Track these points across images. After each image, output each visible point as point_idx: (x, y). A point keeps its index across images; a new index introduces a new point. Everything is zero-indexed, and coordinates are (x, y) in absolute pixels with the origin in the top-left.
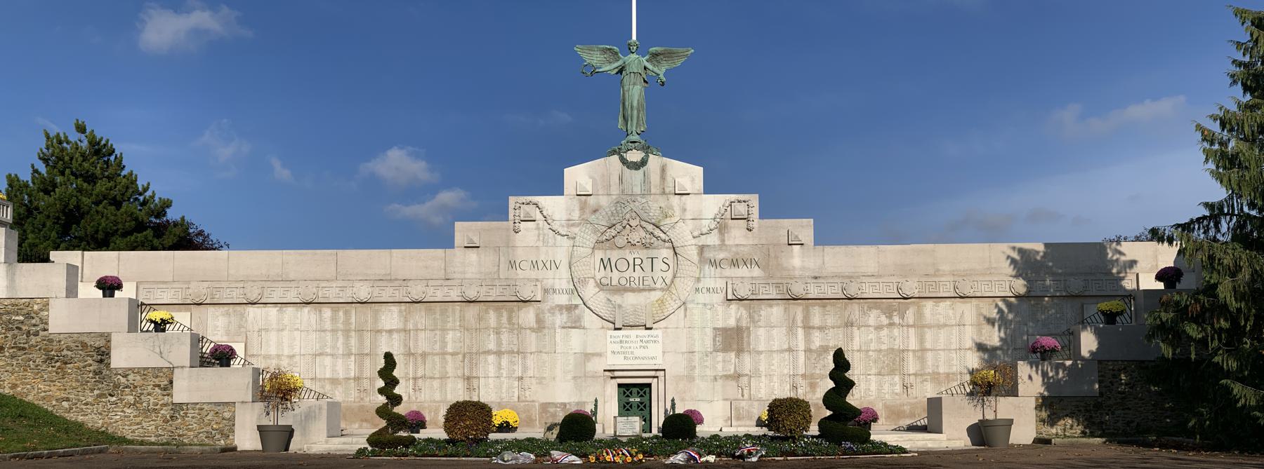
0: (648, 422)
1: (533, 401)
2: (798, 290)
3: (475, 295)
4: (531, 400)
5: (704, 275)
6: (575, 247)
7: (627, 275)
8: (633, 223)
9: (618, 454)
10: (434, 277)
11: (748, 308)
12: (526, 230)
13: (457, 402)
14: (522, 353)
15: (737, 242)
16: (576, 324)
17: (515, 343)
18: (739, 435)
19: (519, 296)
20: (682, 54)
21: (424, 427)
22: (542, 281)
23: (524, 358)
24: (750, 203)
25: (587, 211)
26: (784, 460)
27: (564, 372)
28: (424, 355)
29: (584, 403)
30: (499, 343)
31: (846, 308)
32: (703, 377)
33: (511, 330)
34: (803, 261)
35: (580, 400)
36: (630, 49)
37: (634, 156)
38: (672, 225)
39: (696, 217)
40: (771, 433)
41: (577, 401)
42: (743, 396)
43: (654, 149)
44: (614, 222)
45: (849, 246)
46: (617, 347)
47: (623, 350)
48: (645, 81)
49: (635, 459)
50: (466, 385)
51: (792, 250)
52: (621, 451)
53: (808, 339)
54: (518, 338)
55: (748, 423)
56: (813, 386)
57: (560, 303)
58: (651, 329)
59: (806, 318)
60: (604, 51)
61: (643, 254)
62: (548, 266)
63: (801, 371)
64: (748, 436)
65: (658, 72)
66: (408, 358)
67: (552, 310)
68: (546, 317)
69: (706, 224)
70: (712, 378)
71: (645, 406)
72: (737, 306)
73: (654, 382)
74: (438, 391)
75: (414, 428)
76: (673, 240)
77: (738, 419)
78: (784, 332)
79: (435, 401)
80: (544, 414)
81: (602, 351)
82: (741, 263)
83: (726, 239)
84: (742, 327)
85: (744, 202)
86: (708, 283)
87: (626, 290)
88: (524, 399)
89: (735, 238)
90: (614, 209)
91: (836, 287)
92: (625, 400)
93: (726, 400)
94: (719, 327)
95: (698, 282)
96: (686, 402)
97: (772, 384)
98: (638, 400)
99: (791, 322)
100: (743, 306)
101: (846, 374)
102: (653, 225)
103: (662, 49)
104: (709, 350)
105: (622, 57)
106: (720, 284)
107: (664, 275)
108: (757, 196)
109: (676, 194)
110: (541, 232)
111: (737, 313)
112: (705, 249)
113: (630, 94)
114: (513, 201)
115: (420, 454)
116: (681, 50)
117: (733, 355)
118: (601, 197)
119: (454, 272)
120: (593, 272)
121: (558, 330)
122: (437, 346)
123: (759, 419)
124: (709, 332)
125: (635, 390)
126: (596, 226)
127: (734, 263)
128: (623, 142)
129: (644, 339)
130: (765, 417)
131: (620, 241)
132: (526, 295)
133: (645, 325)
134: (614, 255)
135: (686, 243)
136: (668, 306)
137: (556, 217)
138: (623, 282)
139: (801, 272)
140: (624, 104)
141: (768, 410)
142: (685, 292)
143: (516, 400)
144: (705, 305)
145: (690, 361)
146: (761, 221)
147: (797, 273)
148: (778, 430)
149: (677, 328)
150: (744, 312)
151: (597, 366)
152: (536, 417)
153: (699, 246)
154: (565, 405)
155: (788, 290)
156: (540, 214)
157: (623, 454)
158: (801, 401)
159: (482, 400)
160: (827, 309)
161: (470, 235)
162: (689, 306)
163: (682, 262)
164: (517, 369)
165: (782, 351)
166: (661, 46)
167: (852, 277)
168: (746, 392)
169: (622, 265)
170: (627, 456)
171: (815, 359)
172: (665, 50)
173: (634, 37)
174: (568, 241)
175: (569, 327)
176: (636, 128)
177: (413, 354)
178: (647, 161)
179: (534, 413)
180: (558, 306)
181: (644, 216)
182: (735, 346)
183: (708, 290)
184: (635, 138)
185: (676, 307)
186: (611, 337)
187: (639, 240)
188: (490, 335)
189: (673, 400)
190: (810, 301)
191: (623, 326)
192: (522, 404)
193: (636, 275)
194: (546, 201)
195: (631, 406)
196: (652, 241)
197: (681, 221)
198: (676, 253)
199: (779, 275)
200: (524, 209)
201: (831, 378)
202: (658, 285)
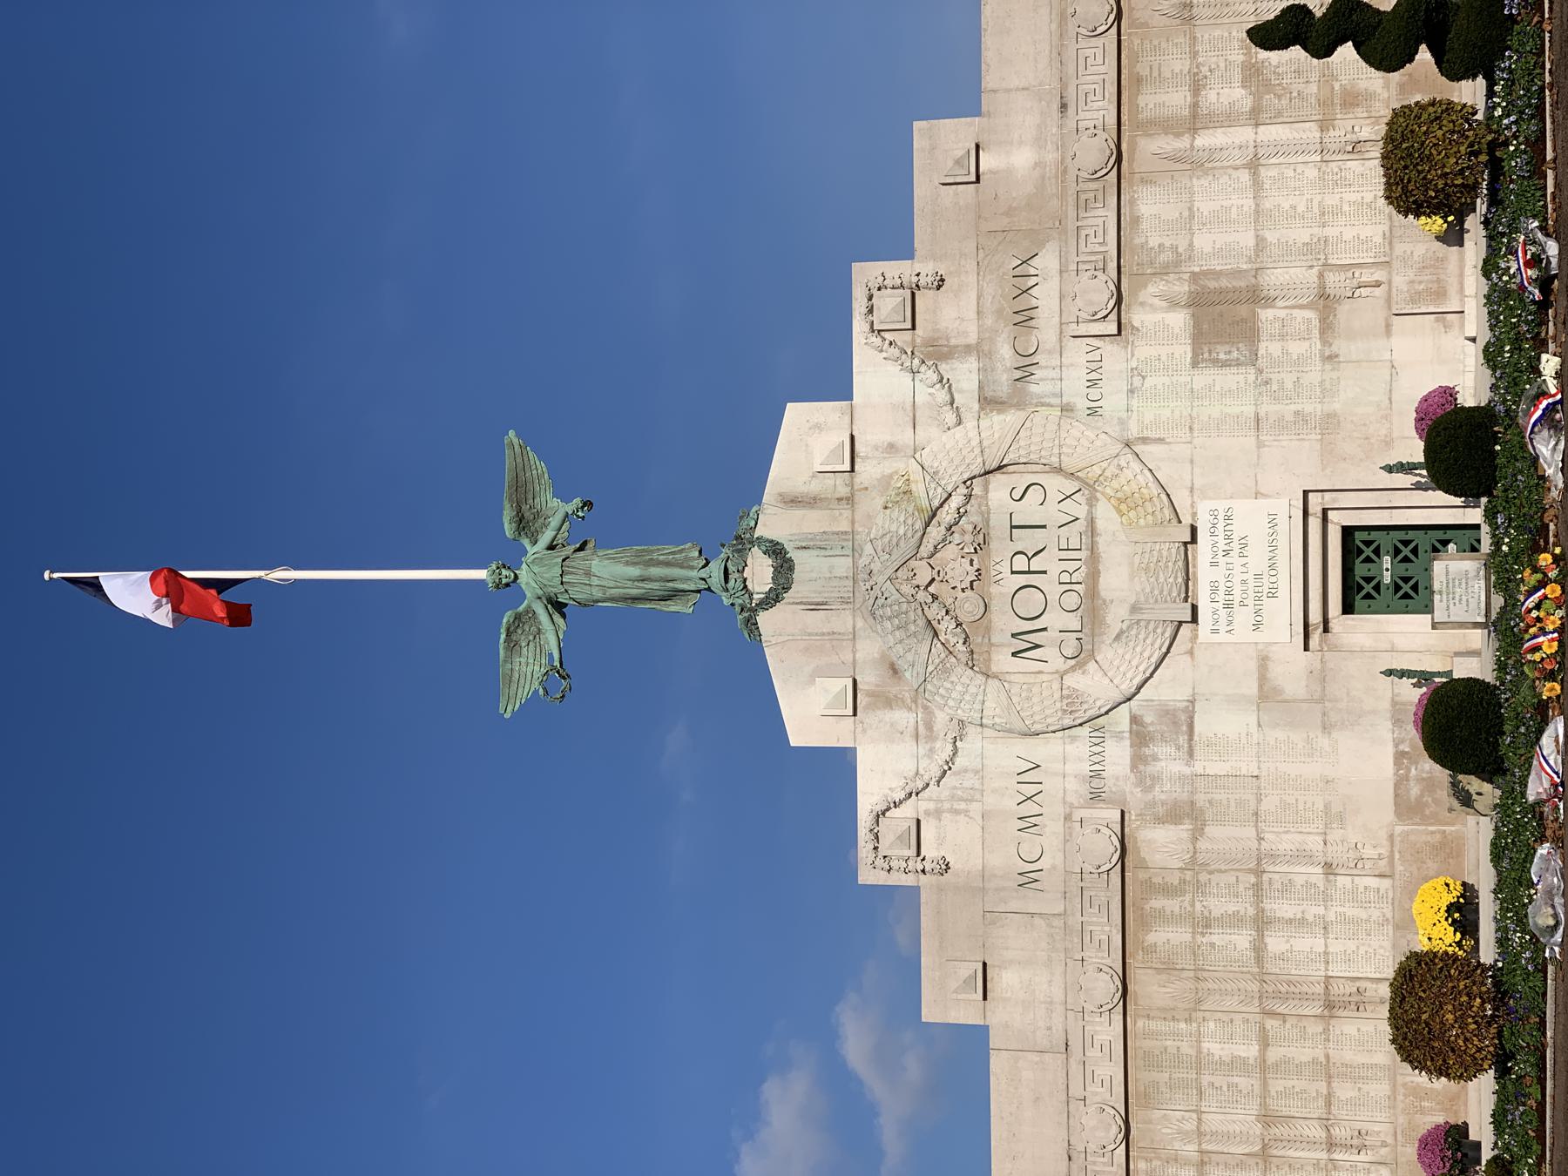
0: (1449, 534)
1: (1391, 837)
2: (1094, 152)
3: (1108, 977)
4: (1386, 843)
5: (1054, 395)
6: (984, 721)
7: (1054, 590)
8: (924, 575)
9: (1538, 619)
10: (1062, 1080)
11: (1142, 279)
12: (941, 841)
13: (1393, 1041)
14: (1259, 860)
15: (972, 315)
16: (1182, 721)
17: (1235, 878)
18: (1485, 290)
19: (1108, 866)
20: (519, 460)
21: (1463, 1130)
22: (1071, 806)
23: (1273, 856)
24: (874, 285)
25: (894, 690)
26: (1554, 169)
27: (1311, 755)
28: (1267, 1118)
29: (1394, 703)
30: (1235, 921)
31: (1145, 25)
32: (1326, 392)
33: (1200, 888)
34: (1021, 143)
35: (1389, 715)
36: (507, 585)
37: (760, 573)
38: (928, 478)
39: (909, 419)
40: (1481, 206)
41: (1389, 725)
42: (1378, 284)
43: (744, 523)
44: (921, 622)
45: (983, 26)
46: (1244, 617)
47: (1250, 602)
48: (581, 548)
49: (1552, 574)
50: (1345, 1014)
51: (991, 172)
52: (1529, 611)
53: (1228, 119)
54: (1220, 871)
55: (1452, 266)
56: (1352, 100)
57: (1128, 761)
58: (1194, 530)
59: (1168, 126)
60: (512, 646)
61: (1001, 549)
62: (1030, 790)
63: (1311, 132)
64: (1489, 268)
65: (559, 516)
66: (1274, 1159)
67: (1147, 782)
68: (1163, 797)
69: (927, 392)
70: (1328, 367)
71: (1406, 543)
73: (1338, 520)
74: (1365, 1088)
75: (1465, 1155)
76: (966, 476)
77: (1440, 294)
78: (1204, 182)
79: (1393, 1097)
80: (1427, 812)
81: (1255, 655)
82: (1022, 303)
83: (961, 341)
84: (1191, 292)
85: (870, 298)
86: (1074, 386)
87: (1093, 593)
88: (1383, 863)
89: (963, 320)
90: (888, 624)
91: (1089, 52)
92: (1387, 595)
93: (1388, 326)
94: (1189, 355)
95: (1072, 410)
96: (1395, 435)
97: (1346, 208)
98: (1387, 561)
99: (1178, 166)
100: (1134, 293)
101: (1318, 13)
102: (928, 525)
103: (507, 505)
104: (1252, 378)
105: (526, 602)
106: (1077, 353)
107: (1054, 496)
108: (856, 267)
109: (853, 470)
110: (947, 806)
111: (1154, 309)
112: (989, 394)
113: (612, 584)
114: (868, 875)
115: (1535, 1090)
116: (509, 463)
117: (1266, 314)
118: (857, 656)
119: (1049, 1028)
120: (1045, 677)
121: (1198, 768)
122: (1243, 1082)
123: (1443, 238)
124: (1205, 377)
125: (1360, 570)
126: (930, 668)
127: (1024, 319)
128: (727, 602)
129: (1222, 545)
130: (1437, 224)
131: (968, 607)
132: (1107, 847)
133: (1185, 544)
134: (1004, 623)
135: (975, 443)
136: (1135, 487)
137: (908, 767)
138: (1072, 600)
139: (1049, 146)
140: (635, 599)
141: (1417, 216)
142: (1098, 443)
143: (1385, 884)
144: (1131, 391)
145: (1281, 425)
146: (917, 254)
147: (1051, 156)
148: (1473, 189)
149: (1192, 462)
150: (1151, 289)
151: (1292, 667)
152: (1432, 833)
153: (981, 408)
154: (1400, 756)
155: (1095, 176)
156: (903, 806)
157: (1538, 607)
158: (1390, 129)
159: (1390, 973)
160: (1145, 72)
161: (953, 985)
162: (1134, 431)
163: (1022, 452)
164: (1305, 877)
165: (1257, 184)
166: (502, 510)
167: (1063, 18)
168: (1367, 277)
169: (1030, 603)
170: (1545, 597)
171: (1279, 97)
172: (511, 500)
173: (481, 574)
174: (969, 738)
175: (1191, 739)
176: (692, 568)
177: (1264, 1147)
178: (772, 541)
179: (1424, 838)
180: (1134, 767)
181: (906, 548)
182: (1243, 310)
183: (1093, 383)
184: (716, 569)
185: (1136, 466)
186: (1214, 632)
187: (966, 561)
188: (1213, 945)
189: (1389, 469)
190: (1124, 118)
191: (1186, 600)
192: (1399, 868)
193: (1054, 568)
194: (870, 793)
195: (1406, 580)
196: (970, 528)
197: (917, 456)
198: (1000, 468)
199: (1055, 202)
200: (890, 847)
201: (1328, 52)
202: (1081, 511)
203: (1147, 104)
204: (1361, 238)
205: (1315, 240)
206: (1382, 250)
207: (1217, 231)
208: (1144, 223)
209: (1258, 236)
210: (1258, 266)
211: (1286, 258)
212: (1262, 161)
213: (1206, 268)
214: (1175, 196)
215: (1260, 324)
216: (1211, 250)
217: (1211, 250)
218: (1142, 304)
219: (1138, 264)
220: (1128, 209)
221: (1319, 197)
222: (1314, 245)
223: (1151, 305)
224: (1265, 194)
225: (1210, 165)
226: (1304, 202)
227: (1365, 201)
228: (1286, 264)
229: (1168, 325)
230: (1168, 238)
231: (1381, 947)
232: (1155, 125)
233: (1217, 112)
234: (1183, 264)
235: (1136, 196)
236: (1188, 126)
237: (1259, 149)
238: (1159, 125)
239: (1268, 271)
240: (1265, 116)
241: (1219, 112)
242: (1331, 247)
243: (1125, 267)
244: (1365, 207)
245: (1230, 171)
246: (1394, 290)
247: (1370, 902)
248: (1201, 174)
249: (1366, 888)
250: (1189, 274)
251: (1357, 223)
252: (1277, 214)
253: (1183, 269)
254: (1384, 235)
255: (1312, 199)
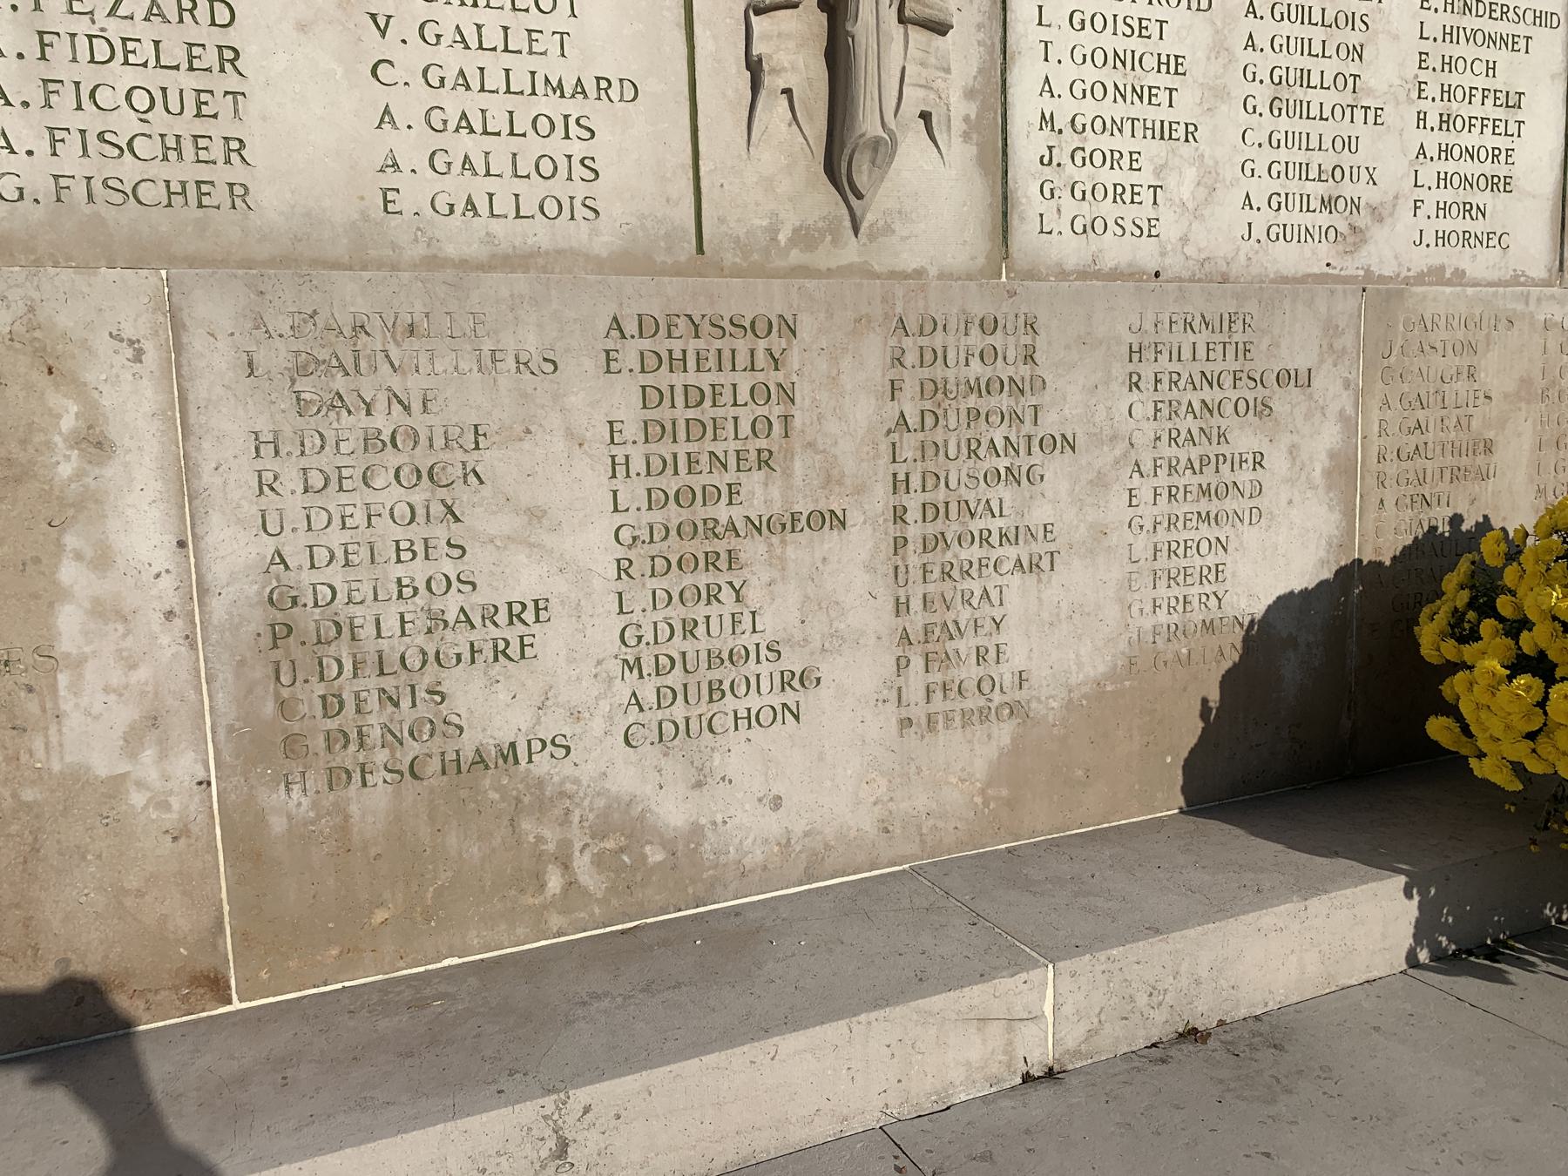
231: (1210, 185)
247: (1446, 121)
249: (1513, 102)
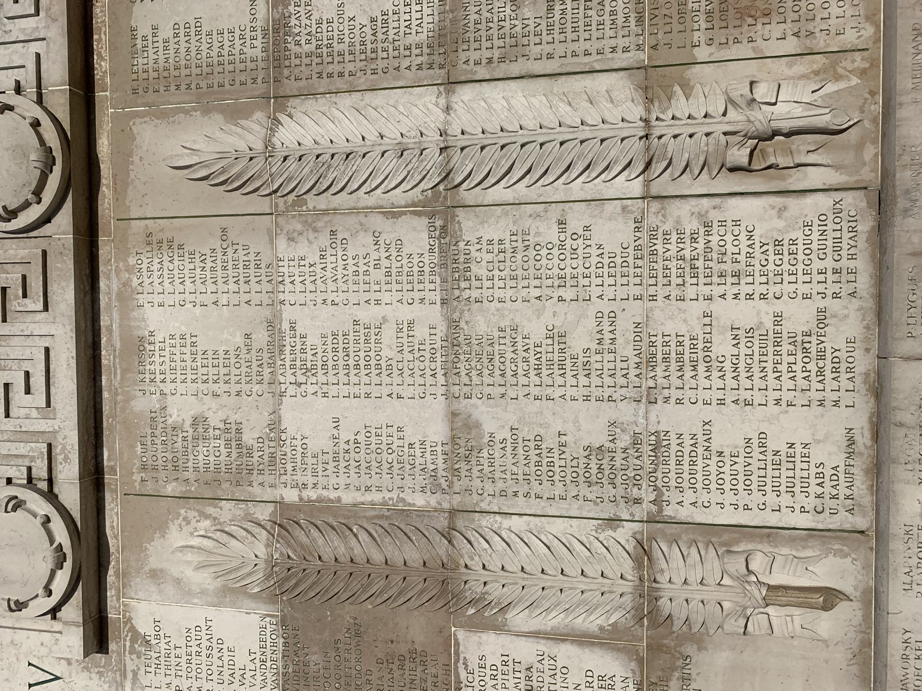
72: (141, 587)
78: (307, 249)
84: (271, 564)
97: (722, 347)
99: (238, 202)
150: (177, 537)
203: (154, 28)
204: (772, 446)
205: (624, 440)
206: (843, 491)
207: (344, 390)
208: (157, 359)
209: (454, 414)
210: (457, 499)
211: (536, 488)
212: (466, 195)
213: (312, 494)
214: (232, 287)
215: (463, 674)
216: (328, 446)
217: (328, 446)
218: (156, 575)
219: (144, 468)
220: (115, 315)
221: (635, 311)
222: (619, 456)
223: (178, 581)
224: (475, 294)
225: (322, 202)
226: (591, 323)
227: (787, 327)
228: (536, 506)
229: (220, 641)
230: (213, 404)
232: (178, 87)
233: (337, 47)
234: (256, 478)
235: (135, 282)
236: (260, 88)
237: (457, 157)
238: (189, 87)
239: (486, 522)
240: (474, 56)
241: (344, 47)
242: (673, 466)
243: (113, 470)
244: (786, 347)
245: (377, 222)
246: (895, 642)
248: (299, 227)
250: (270, 508)
251: (758, 398)
252: (509, 355)
253: (257, 491)
254: (851, 442)
255: (613, 317)
